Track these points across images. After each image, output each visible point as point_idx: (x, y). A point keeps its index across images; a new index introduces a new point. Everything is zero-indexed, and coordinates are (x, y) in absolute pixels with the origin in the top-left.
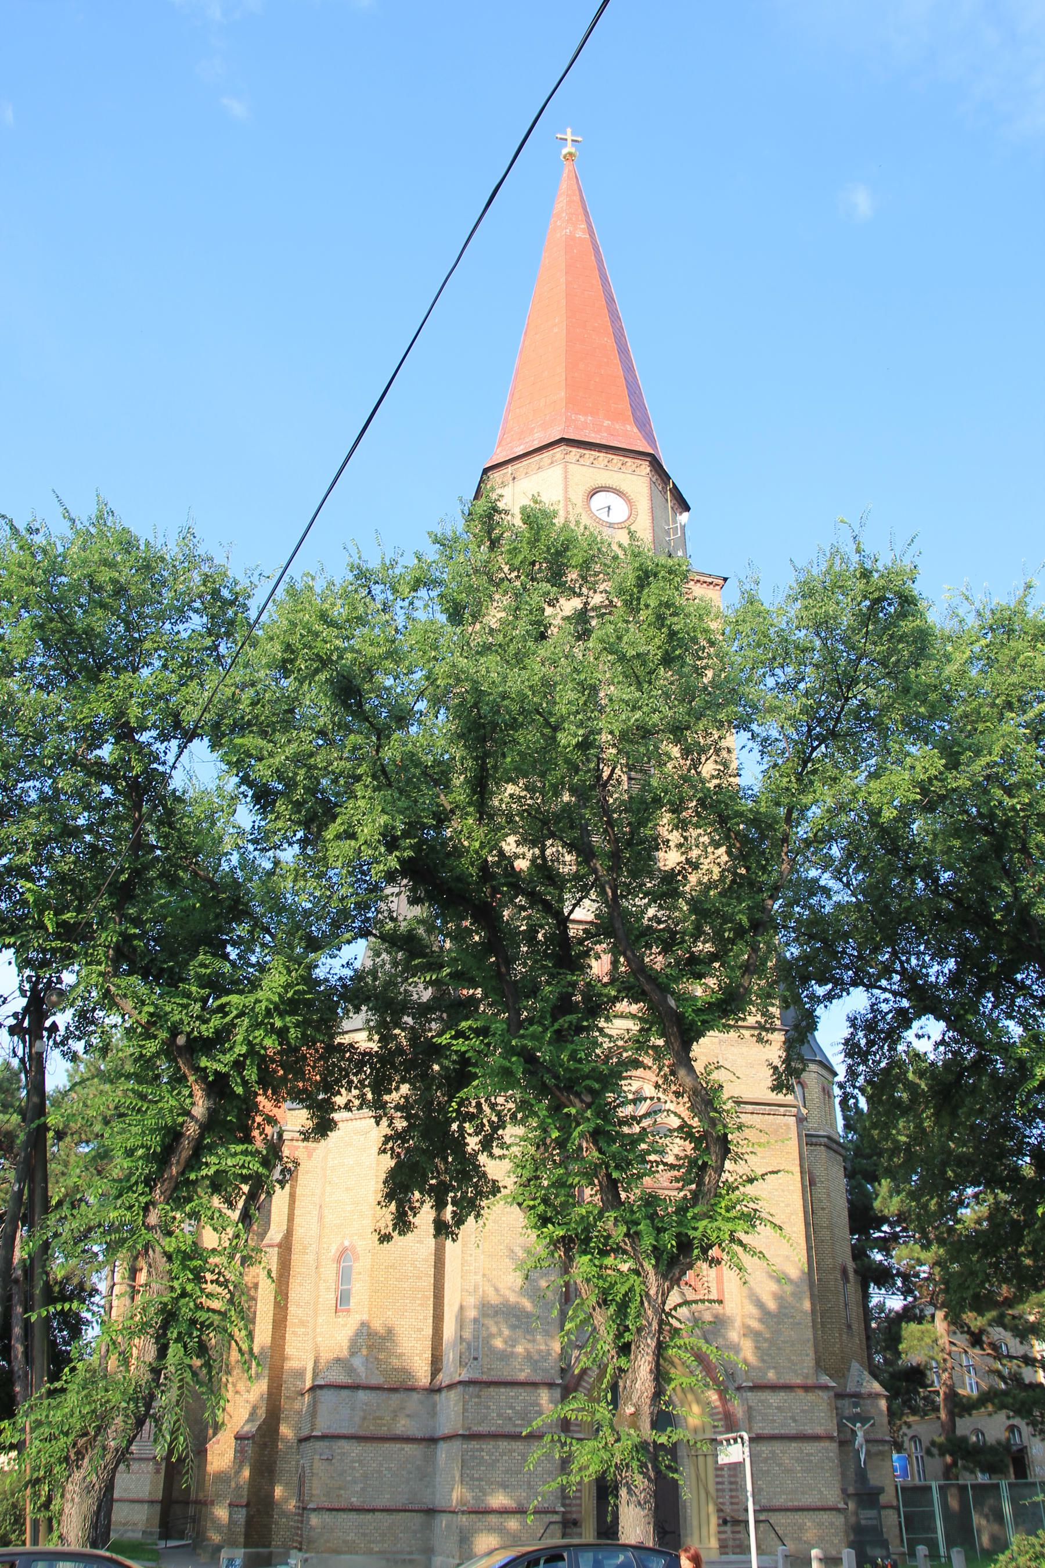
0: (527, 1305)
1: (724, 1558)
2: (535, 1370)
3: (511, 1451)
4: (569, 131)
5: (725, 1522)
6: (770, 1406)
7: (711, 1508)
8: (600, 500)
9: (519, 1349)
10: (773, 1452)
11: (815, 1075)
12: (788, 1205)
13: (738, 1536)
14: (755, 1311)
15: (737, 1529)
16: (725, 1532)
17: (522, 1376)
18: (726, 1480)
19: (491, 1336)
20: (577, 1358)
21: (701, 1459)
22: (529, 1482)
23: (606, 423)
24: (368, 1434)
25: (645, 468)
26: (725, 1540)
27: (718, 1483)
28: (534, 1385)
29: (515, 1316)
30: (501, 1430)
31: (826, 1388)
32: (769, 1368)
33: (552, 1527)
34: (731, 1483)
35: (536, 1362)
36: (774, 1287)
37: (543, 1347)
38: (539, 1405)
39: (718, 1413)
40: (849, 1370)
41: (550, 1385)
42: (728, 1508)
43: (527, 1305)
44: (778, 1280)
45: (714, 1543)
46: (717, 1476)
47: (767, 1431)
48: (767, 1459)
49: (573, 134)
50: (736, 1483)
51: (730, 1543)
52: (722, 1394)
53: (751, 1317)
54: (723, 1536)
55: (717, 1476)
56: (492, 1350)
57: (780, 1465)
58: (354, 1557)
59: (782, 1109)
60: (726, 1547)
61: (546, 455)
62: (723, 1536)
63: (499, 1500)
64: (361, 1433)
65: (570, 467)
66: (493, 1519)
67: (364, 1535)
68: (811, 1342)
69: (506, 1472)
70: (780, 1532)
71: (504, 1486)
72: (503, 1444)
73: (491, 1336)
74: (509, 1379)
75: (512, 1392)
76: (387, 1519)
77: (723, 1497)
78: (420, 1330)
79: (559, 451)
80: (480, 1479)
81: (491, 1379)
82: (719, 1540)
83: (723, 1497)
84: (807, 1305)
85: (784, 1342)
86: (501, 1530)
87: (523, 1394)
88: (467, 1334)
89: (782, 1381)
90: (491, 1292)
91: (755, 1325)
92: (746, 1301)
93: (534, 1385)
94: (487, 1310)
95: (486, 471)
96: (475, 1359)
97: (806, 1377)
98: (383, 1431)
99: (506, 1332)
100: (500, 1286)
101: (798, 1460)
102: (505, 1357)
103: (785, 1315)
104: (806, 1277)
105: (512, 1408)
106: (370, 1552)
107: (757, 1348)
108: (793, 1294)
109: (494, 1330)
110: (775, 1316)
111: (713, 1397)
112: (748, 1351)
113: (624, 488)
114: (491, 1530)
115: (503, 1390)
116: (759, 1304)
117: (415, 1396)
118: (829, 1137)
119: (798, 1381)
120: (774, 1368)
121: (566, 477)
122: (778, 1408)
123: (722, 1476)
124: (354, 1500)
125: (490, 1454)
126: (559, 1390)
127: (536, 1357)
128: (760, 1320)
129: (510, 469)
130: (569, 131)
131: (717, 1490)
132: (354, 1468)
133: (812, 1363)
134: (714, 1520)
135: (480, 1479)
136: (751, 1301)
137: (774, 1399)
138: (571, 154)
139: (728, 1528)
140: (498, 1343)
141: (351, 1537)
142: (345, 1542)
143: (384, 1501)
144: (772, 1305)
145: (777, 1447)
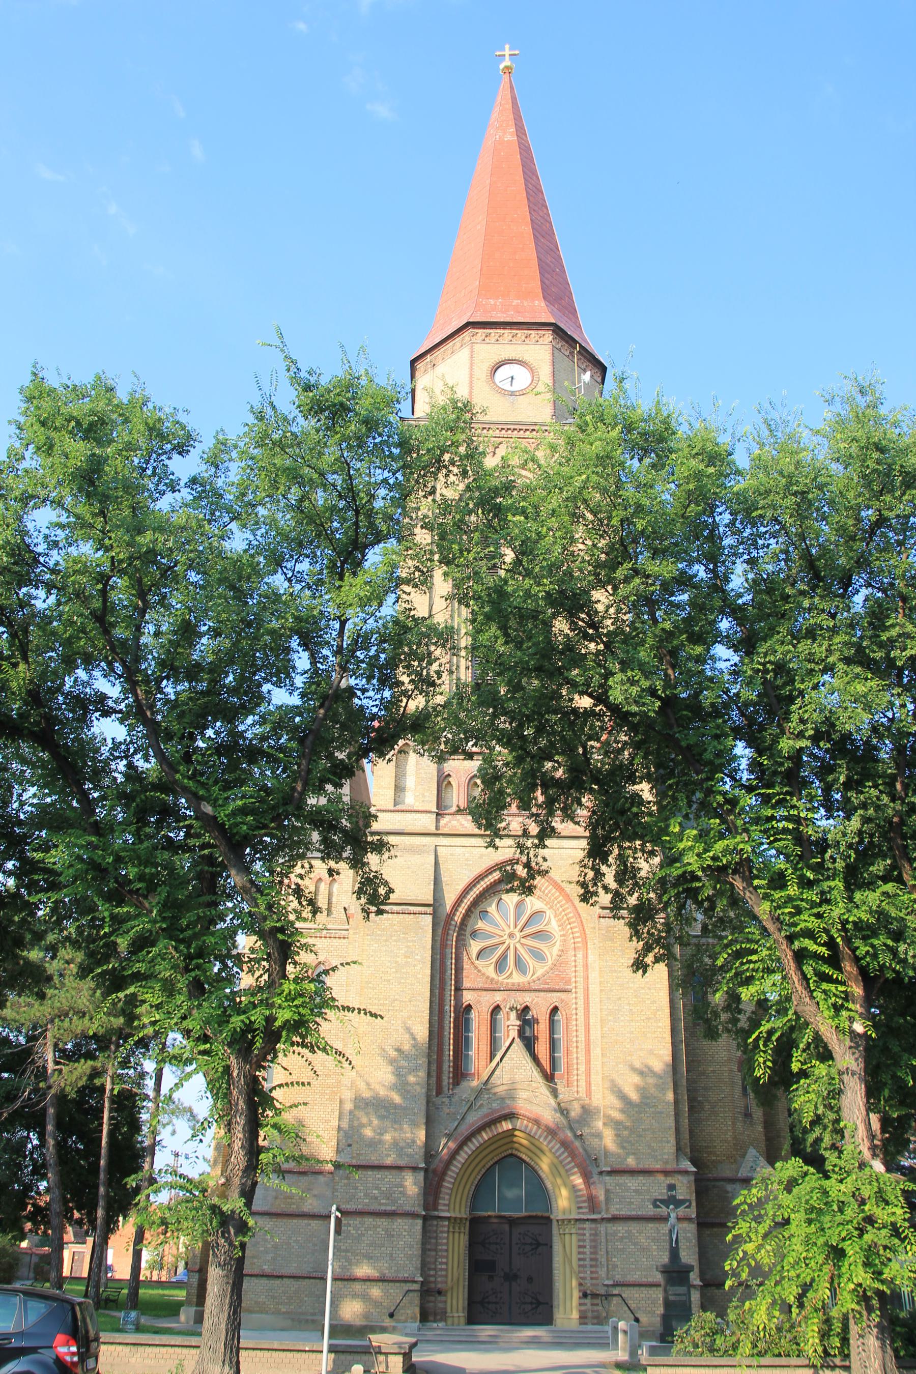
0: (397, 1099)
1: (583, 1328)
2: (400, 1155)
3: (376, 1227)
4: (507, 47)
5: (585, 1295)
6: (628, 1189)
7: (574, 1283)
8: (504, 373)
9: (388, 1137)
10: (629, 1232)
12: (654, 1002)
13: (595, 1308)
15: (596, 1301)
16: (585, 1304)
17: (389, 1161)
18: (588, 1256)
19: (362, 1126)
20: (445, 1145)
21: (567, 1237)
22: (391, 1255)
23: (515, 302)
24: (279, 1211)
25: (548, 336)
26: (585, 1311)
27: (580, 1259)
28: (399, 1168)
29: (385, 1107)
30: (366, 1209)
31: (686, 1172)
32: (628, 1154)
33: (411, 1294)
34: (592, 1259)
35: (402, 1148)
36: (636, 1079)
37: (408, 1135)
38: (402, 1186)
39: (582, 1196)
40: (743, 1156)
41: (414, 1169)
42: (588, 1282)
43: (397, 1099)
44: (641, 1073)
45: (575, 1315)
46: (579, 1253)
47: (624, 1212)
48: (622, 1238)
49: (510, 49)
50: (596, 1260)
51: (589, 1314)
52: (586, 1176)
54: (583, 1308)
55: (579, 1253)
56: (361, 1137)
57: (635, 1244)
58: (264, 1316)
60: (585, 1317)
61: (458, 340)
62: (583, 1308)
63: (363, 1270)
64: (274, 1210)
65: (476, 347)
66: (358, 1287)
67: (273, 1297)
68: (673, 1130)
69: (370, 1245)
70: (633, 1306)
71: (369, 1257)
72: (369, 1221)
73: (362, 1126)
74: (376, 1163)
75: (379, 1175)
76: (293, 1285)
77: (585, 1272)
78: (328, 1121)
79: (467, 335)
80: (347, 1251)
81: (360, 1163)
82: (580, 1311)
83: (585, 1272)
84: (670, 1096)
85: (644, 1130)
86: (365, 1297)
87: (389, 1176)
88: (345, 1125)
89: (641, 1166)
90: (362, 1086)
91: (617, 1115)
92: (607, 1093)
93: (399, 1168)
94: (361, 1103)
95: (413, 362)
96: (350, 1145)
97: (666, 1163)
98: (293, 1208)
99: (376, 1122)
100: (371, 1081)
101: (654, 1240)
102: (373, 1144)
103: (646, 1104)
104: (670, 1069)
105: (377, 1188)
106: (277, 1312)
107: (617, 1135)
108: (656, 1086)
109: (364, 1120)
110: (637, 1105)
111: (578, 1181)
112: (609, 1140)
113: (527, 358)
114: (355, 1296)
115: (370, 1173)
116: (623, 1097)
117: (321, 1179)
119: (658, 1166)
120: (633, 1154)
121: (472, 357)
122: (635, 1191)
123: (584, 1253)
124: (265, 1267)
125: (356, 1228)
126: (422, 1174)
127: (402, 1144)
129: (429, 358)
130: (507, 47)
131: (580, 1266)
132: (266, 1240)
133: (673, 1150)
134: (576, 1294)
135: (347, 1251)
136: (613, 1091)
137: (632, 1183)
138: (507, 67)
139: (588, 1301)
140: (368, 1132)
141: (262, 1299)
142: (256, 1302)
143: (292, 1269)
144: (634, 1096)
145: (634, 1227)
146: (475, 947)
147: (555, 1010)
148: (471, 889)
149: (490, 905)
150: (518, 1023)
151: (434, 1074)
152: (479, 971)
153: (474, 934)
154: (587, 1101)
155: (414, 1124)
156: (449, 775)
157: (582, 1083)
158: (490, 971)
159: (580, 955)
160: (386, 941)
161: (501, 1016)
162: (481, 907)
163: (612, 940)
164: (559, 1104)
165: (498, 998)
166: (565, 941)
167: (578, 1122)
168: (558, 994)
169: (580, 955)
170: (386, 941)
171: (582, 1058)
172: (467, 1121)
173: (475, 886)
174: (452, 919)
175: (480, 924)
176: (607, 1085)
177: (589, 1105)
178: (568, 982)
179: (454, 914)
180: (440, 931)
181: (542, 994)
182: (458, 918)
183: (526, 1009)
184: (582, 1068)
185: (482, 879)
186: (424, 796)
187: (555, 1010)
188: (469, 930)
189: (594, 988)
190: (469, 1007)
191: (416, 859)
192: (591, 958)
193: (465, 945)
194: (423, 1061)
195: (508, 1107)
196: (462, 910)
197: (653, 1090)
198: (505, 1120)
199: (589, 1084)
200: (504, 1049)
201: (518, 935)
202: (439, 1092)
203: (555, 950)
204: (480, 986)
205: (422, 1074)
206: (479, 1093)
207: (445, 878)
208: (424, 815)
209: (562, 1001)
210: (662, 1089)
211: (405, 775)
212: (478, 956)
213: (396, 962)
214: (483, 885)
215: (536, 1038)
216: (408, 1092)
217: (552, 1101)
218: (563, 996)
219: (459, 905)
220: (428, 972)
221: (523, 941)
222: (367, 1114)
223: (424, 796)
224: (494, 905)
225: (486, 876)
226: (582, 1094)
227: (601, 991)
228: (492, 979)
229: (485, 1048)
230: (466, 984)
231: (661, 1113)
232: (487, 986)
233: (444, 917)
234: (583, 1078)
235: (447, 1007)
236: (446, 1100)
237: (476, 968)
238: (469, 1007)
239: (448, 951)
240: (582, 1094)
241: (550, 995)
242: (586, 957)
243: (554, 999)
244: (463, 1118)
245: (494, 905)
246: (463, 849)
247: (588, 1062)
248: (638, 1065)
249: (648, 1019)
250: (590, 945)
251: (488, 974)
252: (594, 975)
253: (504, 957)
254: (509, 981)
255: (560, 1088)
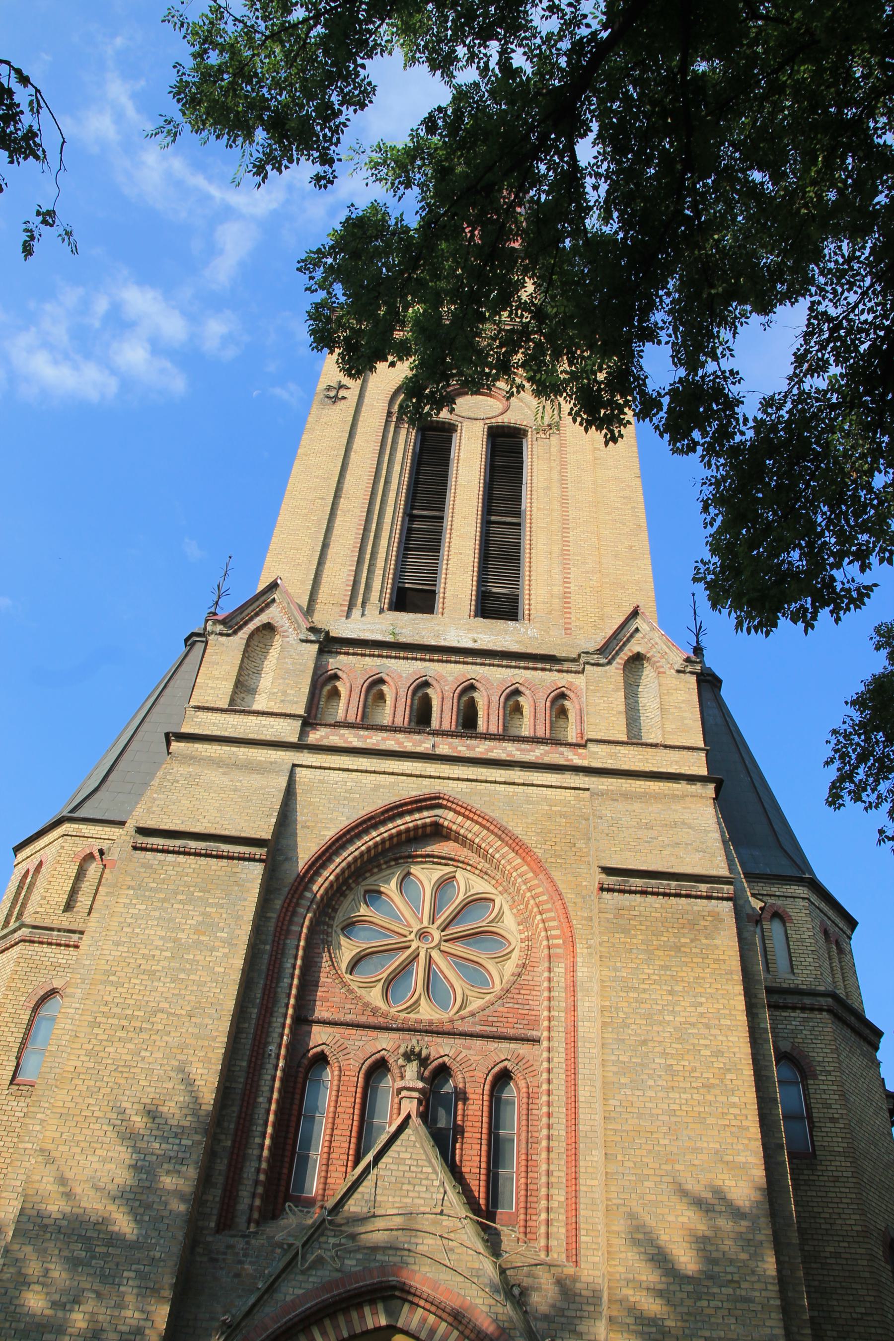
11: (805, 903)
12: (718, 1054)
14: (649, 1276)
29: (86, 1240)
44: (699, 1203)
53: (638, 1285)
59: (703, 887)
90: (47, 1184)
92: (619, 1242)
99: (58, 1273)
100: (69, 1175)
110: (688, 1279)
118: (834, 996)
128: (660, 1294)
136: (635, 1242)
146: (347, 949)
147: (503, 1078)
148: (351, 841)
149: (387, 882)
150: (420, 1085)
151: (219, 1180)
152: (351, 991)
153: (349, 927)
154: (570, 1270)
155: (148, 1290)
156: (336, 677)
157: (559, 1230)
158: (375, 997)
159: (560, 969)
160: (164, 900)
161: (390, 1083)
162: (369, 882)
163: (626, 931)
164: (502, 1271)
165: (385, 1042)
166: (529, 948)
167: (546, 1317)
168: (513, 1046)
169: (560, 969)
170: (164, 900)
171: (560, 1174)
172: (279, 1296)
173: (358, 836)
174: (307, 888)
175: (363, 910)
176: (620, 1225)
177: (575, 1279)
178: (534, 1023)
179: (312, 881)
180: (278, 903)
181: (478, 1043)
182: (319, 886)
183: (443, 1072)
184: (559, 1196)
185: (375, 827)
186: (285, 693)
187: (503, 1078)
188: (340, 918)
189: (588, 1029)
190: (322, 1060)
191: (254, 781)
192: (582, 972)
193: (329, 943)
194: (196, 1142)
195: (383, 1268)
196: (329, 875)
197: (729, 1246)
198: (372, 1302)
199: (574, 1230)
200: (384, 1138)
201: (437, 935)
202: (226, 1222)
203: (510, 967)
204: (349, 1018)
205: (192, 1172)
206: (319, 1228)
207: (303, 814)
208: (281, 720)
209: (520, 1059)
210: (747, 1242)
211: (259, 672)
212: (353, 967)
213: (176, 940)
214: (375, 836)
215: (459, 1131)
216: (148, 1207)
217: (488, 1267)
218: (522, 1049)
219: (324, 866)
220: (238, 962)
221: (445, 946)
222: (42, 1252)
223: (285, 693)
224: (393, 883)
225: (383, 822)
226: (558, 1254)
227: (604, 1024)
228: (375, 1011)
229: (344, 1144)
230: (321, 1011)
231: (748, 1300)
232: (362, 1019)
233: (290, 879)
234: (560, 1218)
235: (273, 1047)
236: (240, 1244)
237: (344, 984)
238: (322, 1060)
239: (291, 942)
240: (558, 1254)
241: (493, 1045)
242: (573, 969)
243: (501, 1052)
244: (271, 1288)
245: (393, 883)
246: (345, 775)
247: (574, 1178)
248: (691, 1185)
249: (708, 1087)
250: (580, 948)
251: (367, 999)
252: (587, 1004)
253: (404, 970)
254: (412, 1015)
255: (509, 1237)
